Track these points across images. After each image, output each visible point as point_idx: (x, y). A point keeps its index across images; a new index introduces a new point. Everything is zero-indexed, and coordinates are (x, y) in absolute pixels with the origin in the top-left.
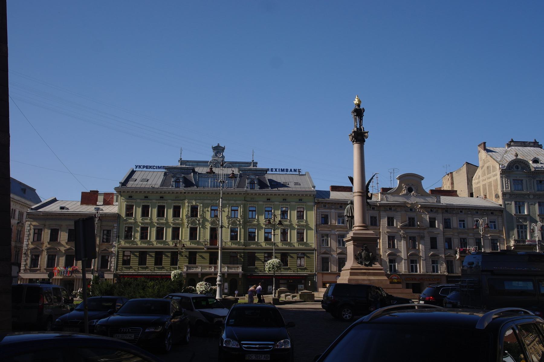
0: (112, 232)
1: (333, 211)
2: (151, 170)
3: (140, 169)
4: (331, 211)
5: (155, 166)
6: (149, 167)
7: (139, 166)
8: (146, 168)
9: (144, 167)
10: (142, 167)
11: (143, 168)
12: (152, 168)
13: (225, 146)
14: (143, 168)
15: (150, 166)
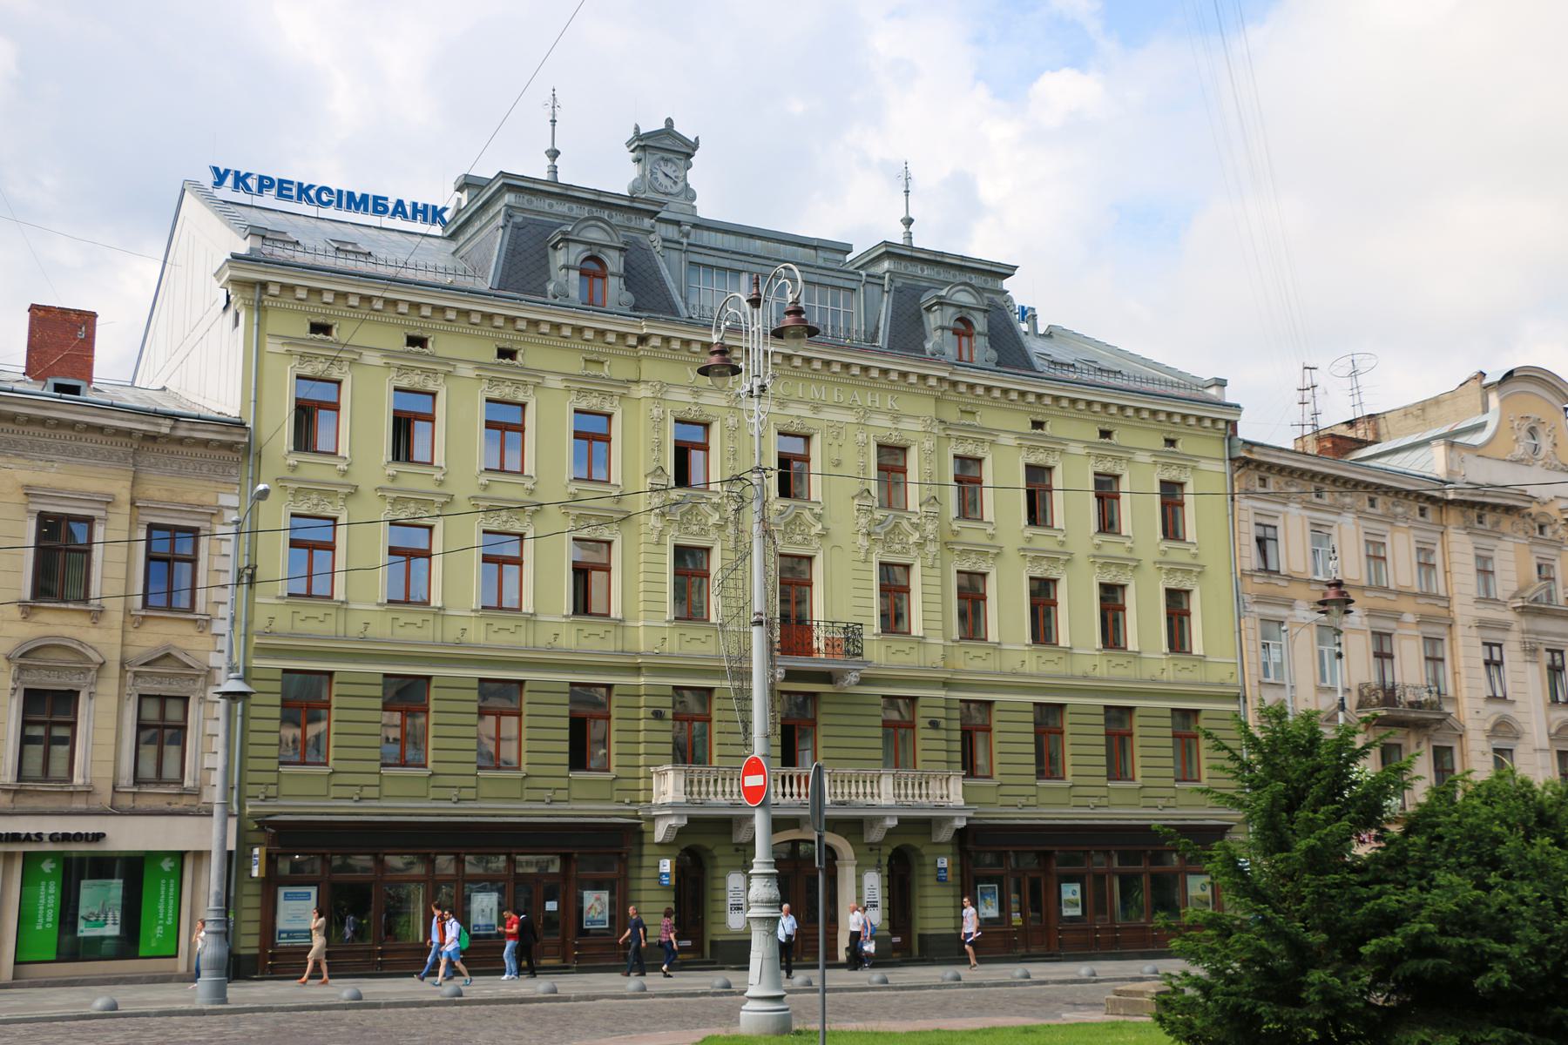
0: (204, 542)
1: (1294, 509)
2: (304, 208)
3: (242, 197)
4: (1286, 509)
5: (330, 191)
6: (294, 193)
7: (237, 173)
8: (280, 195)
9: (265, 183)
10: (253, 183)
11: (260, 191)
12: (310, 200)
13: (697, 139)
14: (260, 191)
15: (300, 185)
